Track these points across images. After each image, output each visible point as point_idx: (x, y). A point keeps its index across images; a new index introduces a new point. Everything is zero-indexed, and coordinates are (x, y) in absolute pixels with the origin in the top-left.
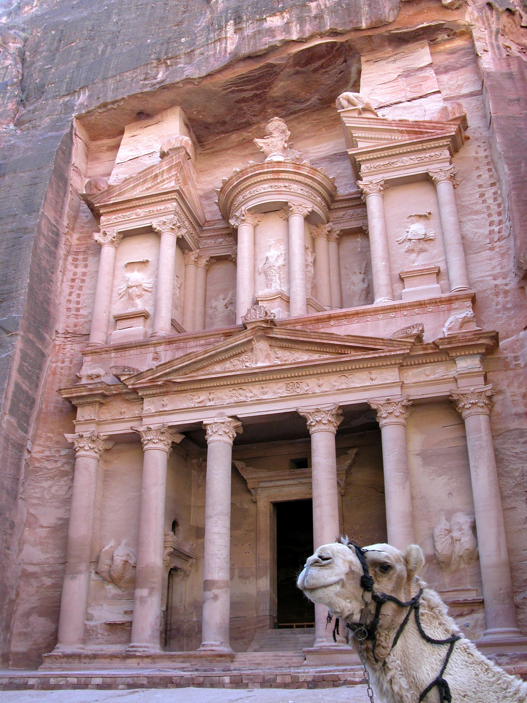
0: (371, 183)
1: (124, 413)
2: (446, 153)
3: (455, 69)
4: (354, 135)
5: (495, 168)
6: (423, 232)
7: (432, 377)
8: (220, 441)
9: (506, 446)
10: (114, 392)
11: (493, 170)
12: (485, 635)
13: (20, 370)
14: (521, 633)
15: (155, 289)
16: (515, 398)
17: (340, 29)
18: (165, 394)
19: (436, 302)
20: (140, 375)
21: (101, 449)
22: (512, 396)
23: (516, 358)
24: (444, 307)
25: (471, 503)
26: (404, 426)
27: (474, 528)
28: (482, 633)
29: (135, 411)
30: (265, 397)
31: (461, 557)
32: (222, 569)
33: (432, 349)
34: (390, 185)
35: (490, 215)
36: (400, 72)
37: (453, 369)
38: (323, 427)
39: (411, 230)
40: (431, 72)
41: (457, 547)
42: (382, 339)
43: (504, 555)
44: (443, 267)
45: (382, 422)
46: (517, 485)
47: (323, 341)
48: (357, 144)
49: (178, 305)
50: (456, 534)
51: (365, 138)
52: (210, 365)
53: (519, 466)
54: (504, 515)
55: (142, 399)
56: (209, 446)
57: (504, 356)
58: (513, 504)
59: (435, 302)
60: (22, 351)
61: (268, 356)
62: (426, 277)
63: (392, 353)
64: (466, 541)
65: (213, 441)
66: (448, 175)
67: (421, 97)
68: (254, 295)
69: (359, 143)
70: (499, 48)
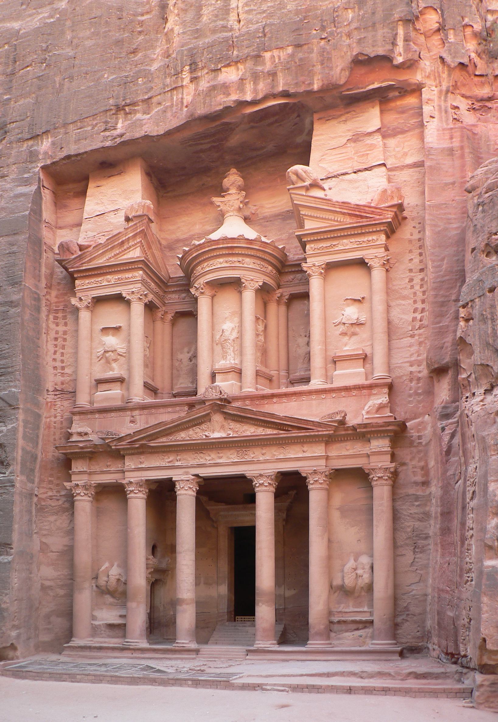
0: (314, 265)
1: (110, 466)
4: (301, 212)
6: (355, 317)
7: (351, 452)
9: (404, 507)
10: (101, 450)
12: (372, 644)
13: (25, 437)
14: (396, 644)
15: (128, 355)
16: (415, 470)
18: (142, 453)
19: (359, 388)
20: (121, 439)
21: (93, 493)
22: (413, 468)
26: (327, 490)
28: (370, 642)
29: (119, 466)
30: (221, 461)
33: (352, 430)
34: (331, 267)
37: (368, 446)
39: (346, 313)
42: (312, 421)
43: (390, 592)
44: (368, 351)
45: (310, 487)
47: (266, 419)
48: (304, 221)
49: (150, 364)
51: (311, 216)
52: (177, 431)
53: (411, 524)
55: (124, 457)
57: (411, 435)
58: (403, 553)
59: (359, 388)
60: (23, 421)
61: (223, 427)
62: (354, 361)
63: (320, 433)
65: (181, 494)
68: (212, 369)
69: (306, 221)
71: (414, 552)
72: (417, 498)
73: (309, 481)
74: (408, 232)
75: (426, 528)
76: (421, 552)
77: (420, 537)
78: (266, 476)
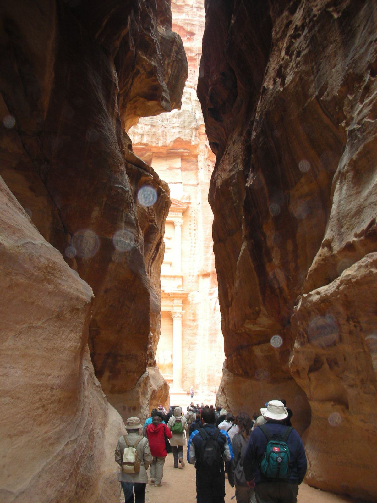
2: (180, 215)
3: (188, 170)
5: (197, 224)
11: (196, 224)
14: (184, 390)
17: (150, 144)
23: (192, 300)
24: (172, 278)
27: (172, 356)
31: (166, 365)
35: (192, 243)
36: (168, 166)
40: (179, 171)
66: (180, 224)
67: (174, 183)
70: (206, 167)
71: (189, 350)
72: (190, 327)
74: (191, 212)
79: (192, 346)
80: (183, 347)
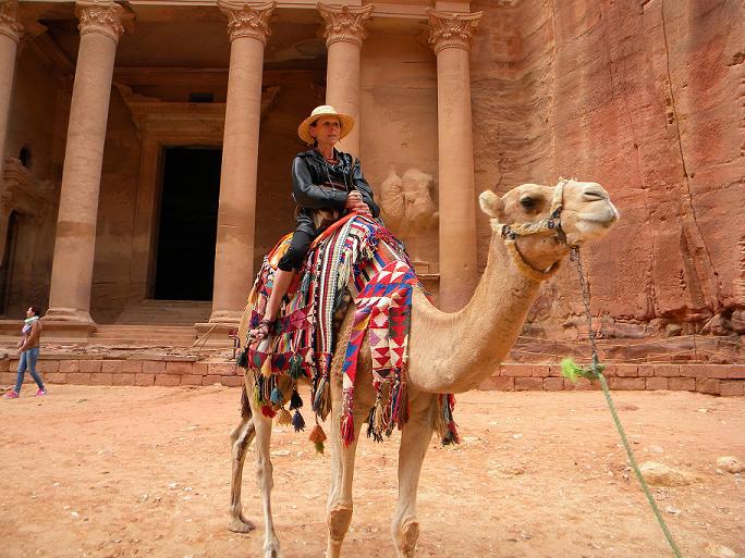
8: (99, 32)
9: (481, 96)
22: (496, 39)
25: (436, 160)
32: (85, 208)
38: (249, 31)
41: (409, 210)
43: (473, 226)
46: (491, 144)
50: (409, 194)
53: (493, 121)
54: (476, 180)
56: (83, 38)
58: (482, 167)
64: (421, 202)
72: (501, 86)
73: (332, 27)
75: (519, 130)
76: (511, 169)
77: (510, 145)
78: (255, 12)
79: (511, 154)
80: (476, 157)
